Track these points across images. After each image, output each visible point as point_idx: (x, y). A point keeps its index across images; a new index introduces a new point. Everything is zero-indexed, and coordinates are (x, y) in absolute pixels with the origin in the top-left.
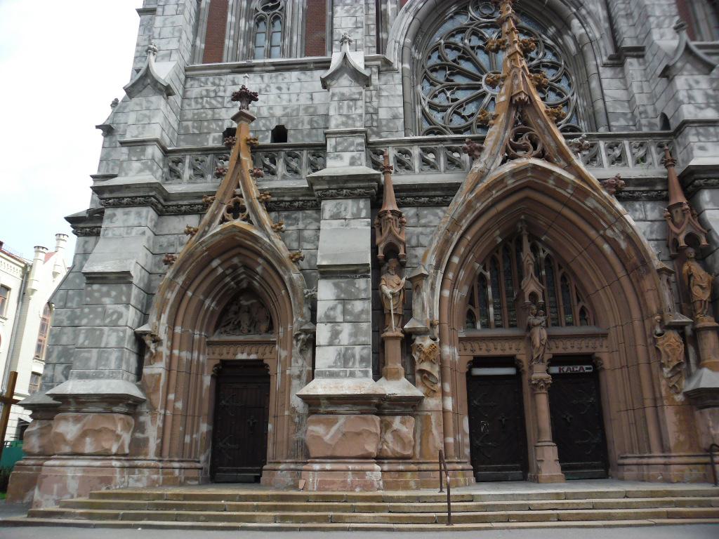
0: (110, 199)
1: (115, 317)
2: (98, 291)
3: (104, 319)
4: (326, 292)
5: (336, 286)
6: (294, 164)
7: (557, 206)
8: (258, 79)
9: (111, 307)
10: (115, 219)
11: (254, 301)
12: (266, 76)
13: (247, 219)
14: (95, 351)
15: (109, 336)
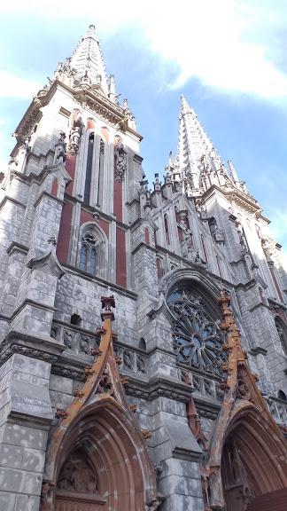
0: (24, 346)
1: (32, 461)
2: (18, 432)
3: (22, 462)
4: (175, 467)
5: (182, 464)
6: (129, 362)
7: (256, 434)
8: (94, 288)
9: (29, 451)
10: (23, 365)
11: (79, 461)
12: (99, 287)
13: (113, 395)
14: (13, 495)
15: (26, 481)
